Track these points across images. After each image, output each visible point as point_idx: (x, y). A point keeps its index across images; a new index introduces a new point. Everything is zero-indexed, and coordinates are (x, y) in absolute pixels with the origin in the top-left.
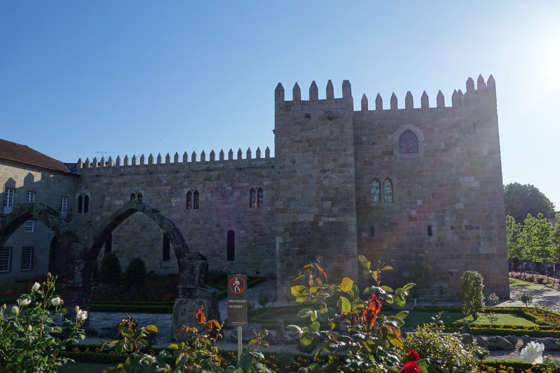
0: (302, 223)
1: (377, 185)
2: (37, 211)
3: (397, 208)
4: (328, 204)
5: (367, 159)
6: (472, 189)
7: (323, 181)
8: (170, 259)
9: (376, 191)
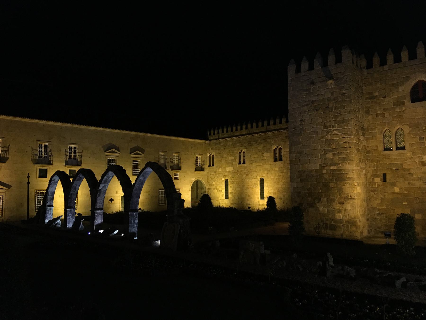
0: (310, 171)
1: (390, 134)
3: (408, 154)
5: (379, 112)
7: (326, 136)
8: (265, 199)
9: (389, 140)
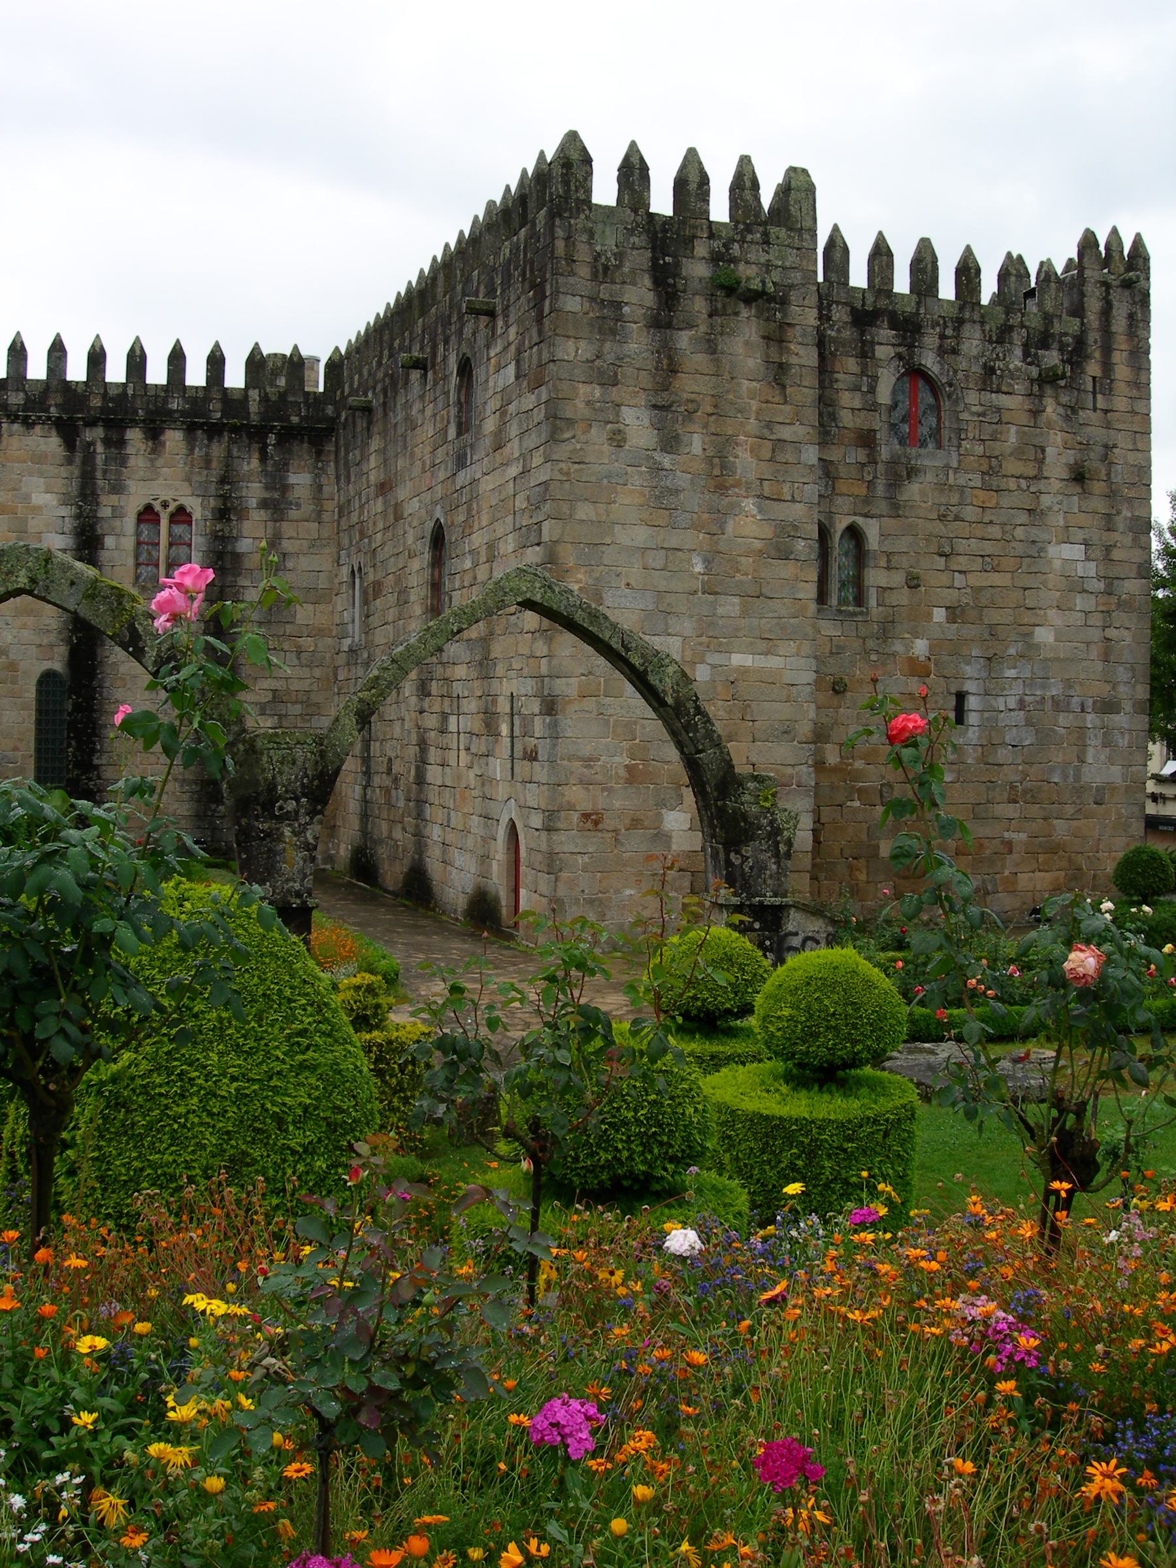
2: (72, 583)
4: (730, 606)
6: (1077, 586)
